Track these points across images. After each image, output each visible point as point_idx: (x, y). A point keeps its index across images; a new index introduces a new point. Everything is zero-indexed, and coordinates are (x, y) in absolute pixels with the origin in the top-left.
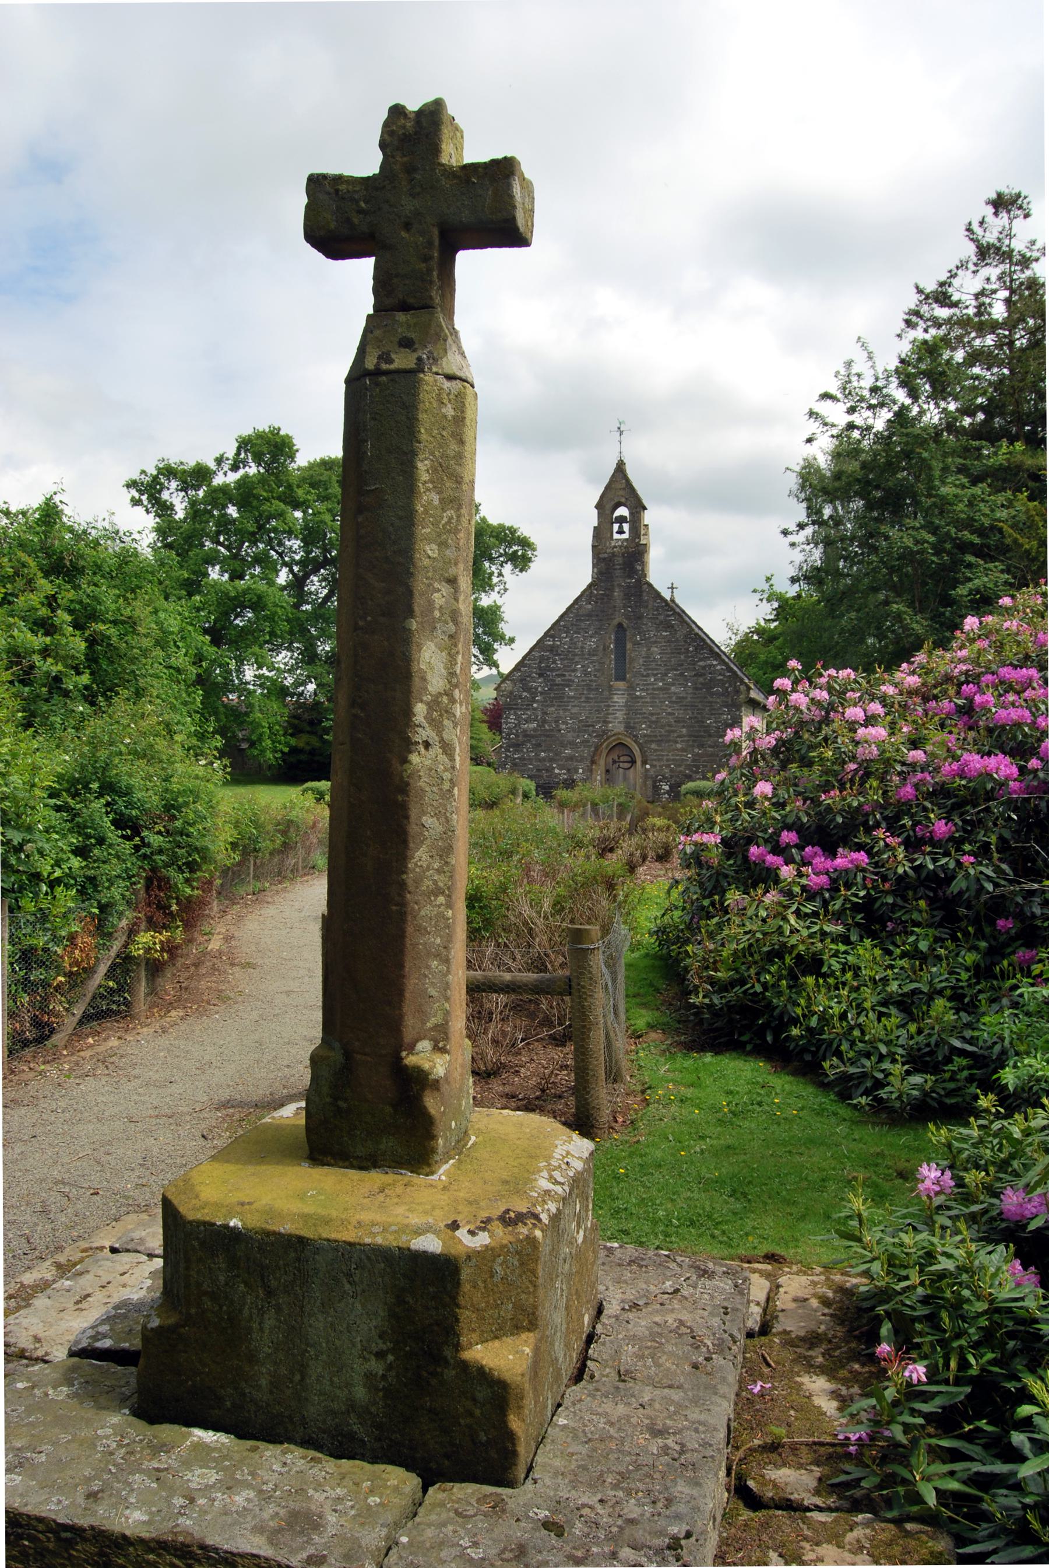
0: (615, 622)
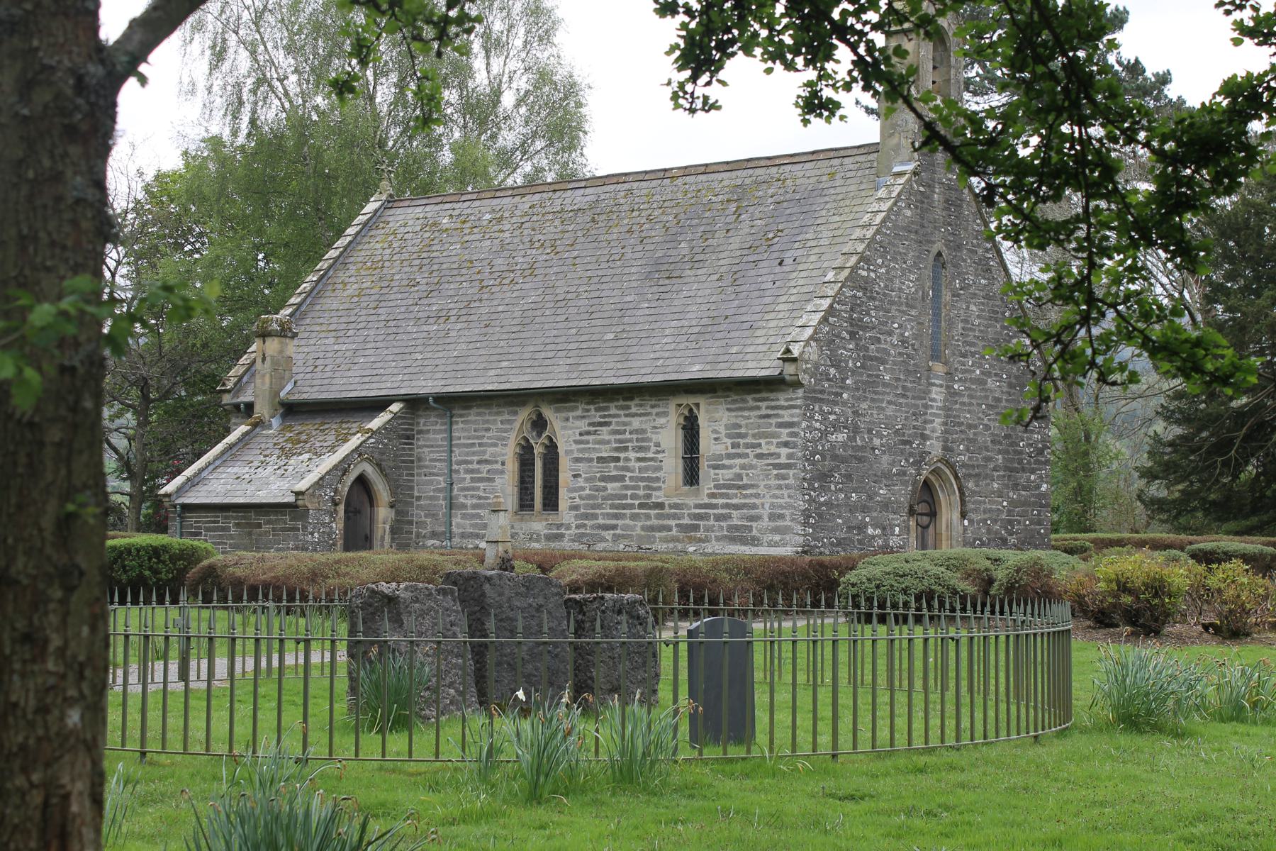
0: (934, 251)
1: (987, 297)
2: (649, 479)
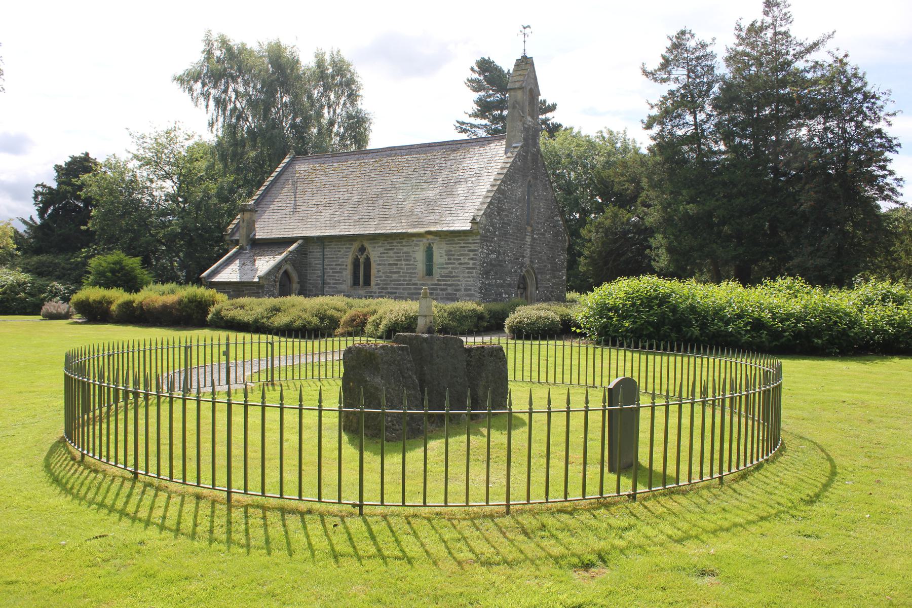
1: (546, 200)
2: (411, 273)
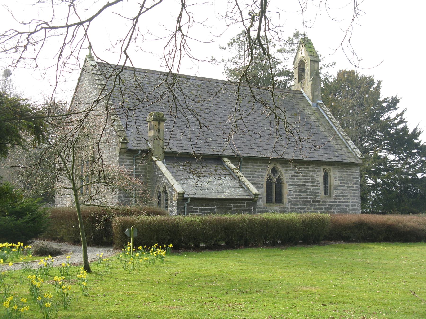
2: (315, 192)
